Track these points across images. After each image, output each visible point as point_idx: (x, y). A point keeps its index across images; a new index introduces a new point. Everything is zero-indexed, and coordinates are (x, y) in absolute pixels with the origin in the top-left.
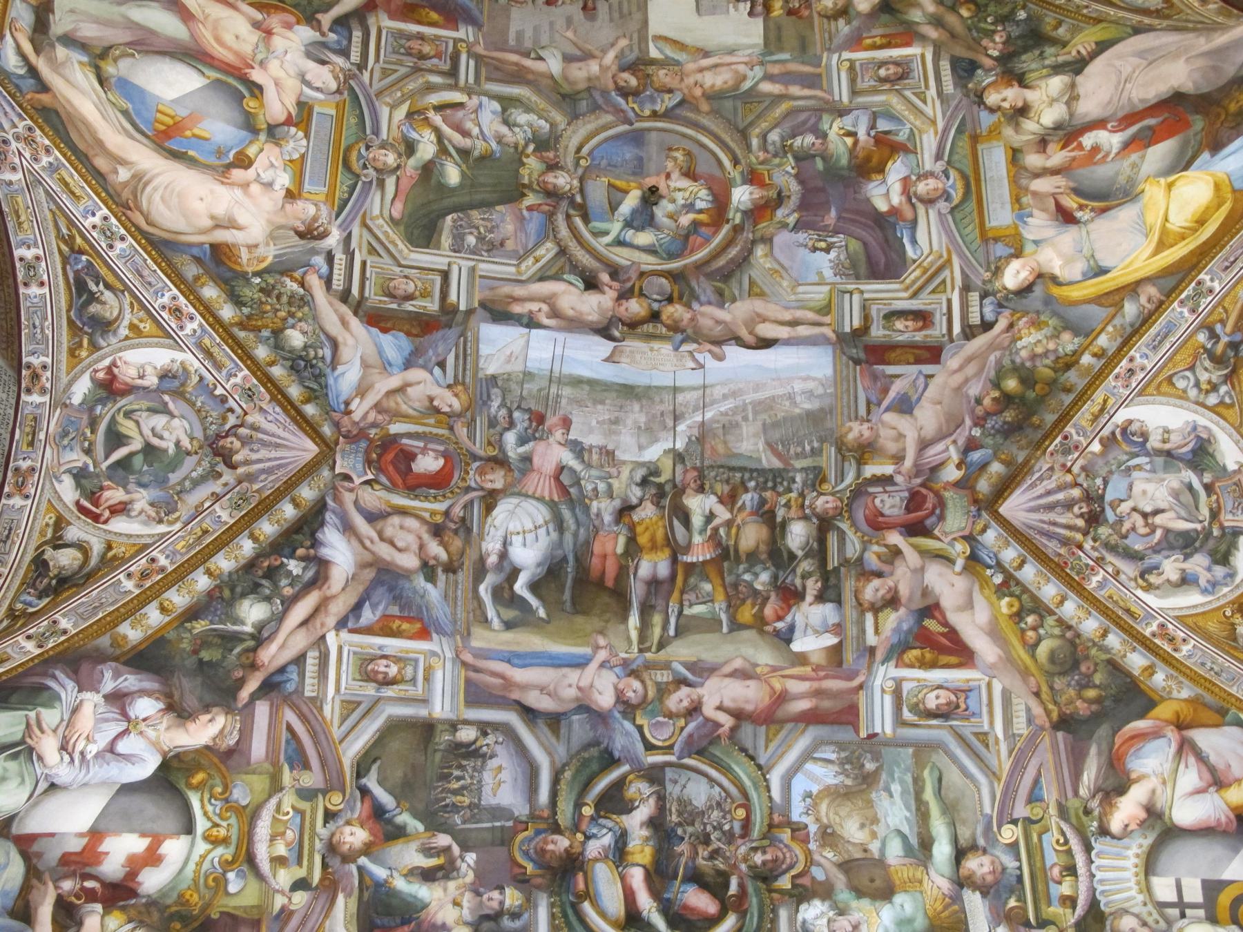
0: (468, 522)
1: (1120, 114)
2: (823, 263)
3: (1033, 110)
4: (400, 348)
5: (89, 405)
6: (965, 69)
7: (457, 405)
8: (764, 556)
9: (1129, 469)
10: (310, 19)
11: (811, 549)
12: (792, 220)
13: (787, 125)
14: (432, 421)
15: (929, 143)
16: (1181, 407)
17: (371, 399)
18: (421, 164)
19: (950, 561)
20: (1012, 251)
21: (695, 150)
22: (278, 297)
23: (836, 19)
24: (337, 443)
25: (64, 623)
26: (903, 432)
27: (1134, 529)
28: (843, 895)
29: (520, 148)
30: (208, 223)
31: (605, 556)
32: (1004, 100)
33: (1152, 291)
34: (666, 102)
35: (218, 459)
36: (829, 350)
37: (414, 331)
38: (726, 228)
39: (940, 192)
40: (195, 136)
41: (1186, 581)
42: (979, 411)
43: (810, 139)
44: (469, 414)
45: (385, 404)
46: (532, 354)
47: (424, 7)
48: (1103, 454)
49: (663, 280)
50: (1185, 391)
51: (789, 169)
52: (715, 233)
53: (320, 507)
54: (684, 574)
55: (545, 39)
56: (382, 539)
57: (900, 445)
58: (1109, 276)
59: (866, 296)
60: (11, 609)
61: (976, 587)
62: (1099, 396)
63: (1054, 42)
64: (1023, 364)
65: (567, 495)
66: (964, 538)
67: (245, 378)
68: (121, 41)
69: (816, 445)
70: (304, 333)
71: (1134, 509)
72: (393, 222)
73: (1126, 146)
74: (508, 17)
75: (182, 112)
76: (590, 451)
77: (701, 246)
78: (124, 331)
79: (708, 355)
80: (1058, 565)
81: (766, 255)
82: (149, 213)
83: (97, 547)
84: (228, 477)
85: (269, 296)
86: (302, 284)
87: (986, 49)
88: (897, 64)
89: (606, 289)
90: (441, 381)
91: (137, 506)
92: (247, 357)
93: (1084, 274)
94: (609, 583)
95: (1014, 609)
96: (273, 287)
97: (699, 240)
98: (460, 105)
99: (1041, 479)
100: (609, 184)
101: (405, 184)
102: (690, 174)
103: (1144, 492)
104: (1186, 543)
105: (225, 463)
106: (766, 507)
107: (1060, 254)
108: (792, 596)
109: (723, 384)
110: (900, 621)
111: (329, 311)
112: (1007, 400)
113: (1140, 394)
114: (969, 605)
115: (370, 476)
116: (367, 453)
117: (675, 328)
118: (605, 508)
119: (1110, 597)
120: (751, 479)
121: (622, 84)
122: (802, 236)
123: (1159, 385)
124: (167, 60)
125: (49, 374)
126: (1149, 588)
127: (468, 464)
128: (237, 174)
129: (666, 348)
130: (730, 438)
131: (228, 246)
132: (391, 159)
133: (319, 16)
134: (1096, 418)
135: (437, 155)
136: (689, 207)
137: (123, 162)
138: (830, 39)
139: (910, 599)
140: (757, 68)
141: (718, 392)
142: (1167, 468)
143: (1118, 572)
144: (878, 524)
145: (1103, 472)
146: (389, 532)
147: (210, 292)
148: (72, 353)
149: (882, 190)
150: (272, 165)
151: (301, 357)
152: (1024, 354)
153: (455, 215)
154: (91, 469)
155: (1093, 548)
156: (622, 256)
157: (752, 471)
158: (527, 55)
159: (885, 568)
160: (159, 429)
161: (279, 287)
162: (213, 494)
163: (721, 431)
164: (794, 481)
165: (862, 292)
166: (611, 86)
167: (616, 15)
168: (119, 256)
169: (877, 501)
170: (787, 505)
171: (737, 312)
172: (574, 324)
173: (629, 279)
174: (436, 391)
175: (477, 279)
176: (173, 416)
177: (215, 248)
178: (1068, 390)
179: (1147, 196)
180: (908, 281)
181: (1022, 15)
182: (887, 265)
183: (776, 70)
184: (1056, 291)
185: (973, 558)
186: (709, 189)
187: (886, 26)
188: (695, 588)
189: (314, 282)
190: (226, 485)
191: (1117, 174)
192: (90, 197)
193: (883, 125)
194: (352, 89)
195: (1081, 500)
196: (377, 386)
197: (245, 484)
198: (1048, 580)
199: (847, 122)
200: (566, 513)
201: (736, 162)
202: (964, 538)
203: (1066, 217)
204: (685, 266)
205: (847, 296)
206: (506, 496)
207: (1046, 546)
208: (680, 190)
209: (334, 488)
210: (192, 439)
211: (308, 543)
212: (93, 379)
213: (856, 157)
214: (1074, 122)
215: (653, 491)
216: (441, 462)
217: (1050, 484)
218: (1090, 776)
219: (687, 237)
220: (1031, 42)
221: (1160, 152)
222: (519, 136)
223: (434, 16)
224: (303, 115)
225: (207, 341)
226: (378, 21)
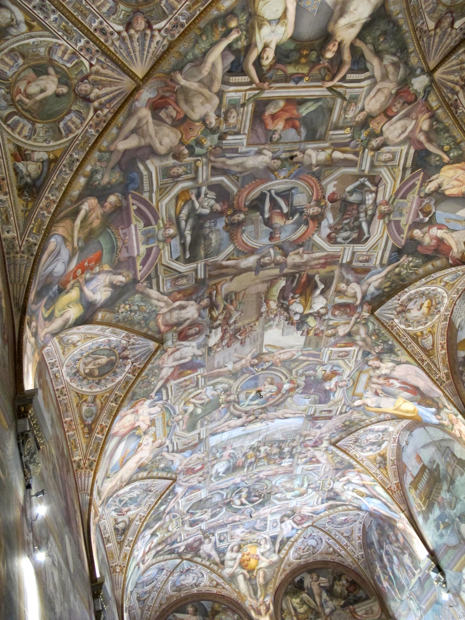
6: (366, 354)
10: (148, 397)
15: (347, 372)
25: (131, 539)
28: (284, 492)
38: (280, 395)
41: (371, 450)
43: (311, 372)
54: (258, 459)
60: (118, 542)
73: (400, 388)
83: (127, 520)
84: (151, 493)
101: (185, 420)
102: (271, 384)
104: (374, 444)
108: (282, 458)
114: (323, 456)
117: (262, 419)
122: (302, 395)
126: (362, 451)
136: (270, 392)
147: (141, 475)
156: (248, 408)
158: (221, 368)
167: (252, 342)
171: (280, 412)
183: (305, 353)
184: (366, 408)
193: (335, 368)
199: (324, 368)
201: (287, 378)
203: (377, 394)
218: (338, 475)
223: (189, 372)
224: (153, 422)
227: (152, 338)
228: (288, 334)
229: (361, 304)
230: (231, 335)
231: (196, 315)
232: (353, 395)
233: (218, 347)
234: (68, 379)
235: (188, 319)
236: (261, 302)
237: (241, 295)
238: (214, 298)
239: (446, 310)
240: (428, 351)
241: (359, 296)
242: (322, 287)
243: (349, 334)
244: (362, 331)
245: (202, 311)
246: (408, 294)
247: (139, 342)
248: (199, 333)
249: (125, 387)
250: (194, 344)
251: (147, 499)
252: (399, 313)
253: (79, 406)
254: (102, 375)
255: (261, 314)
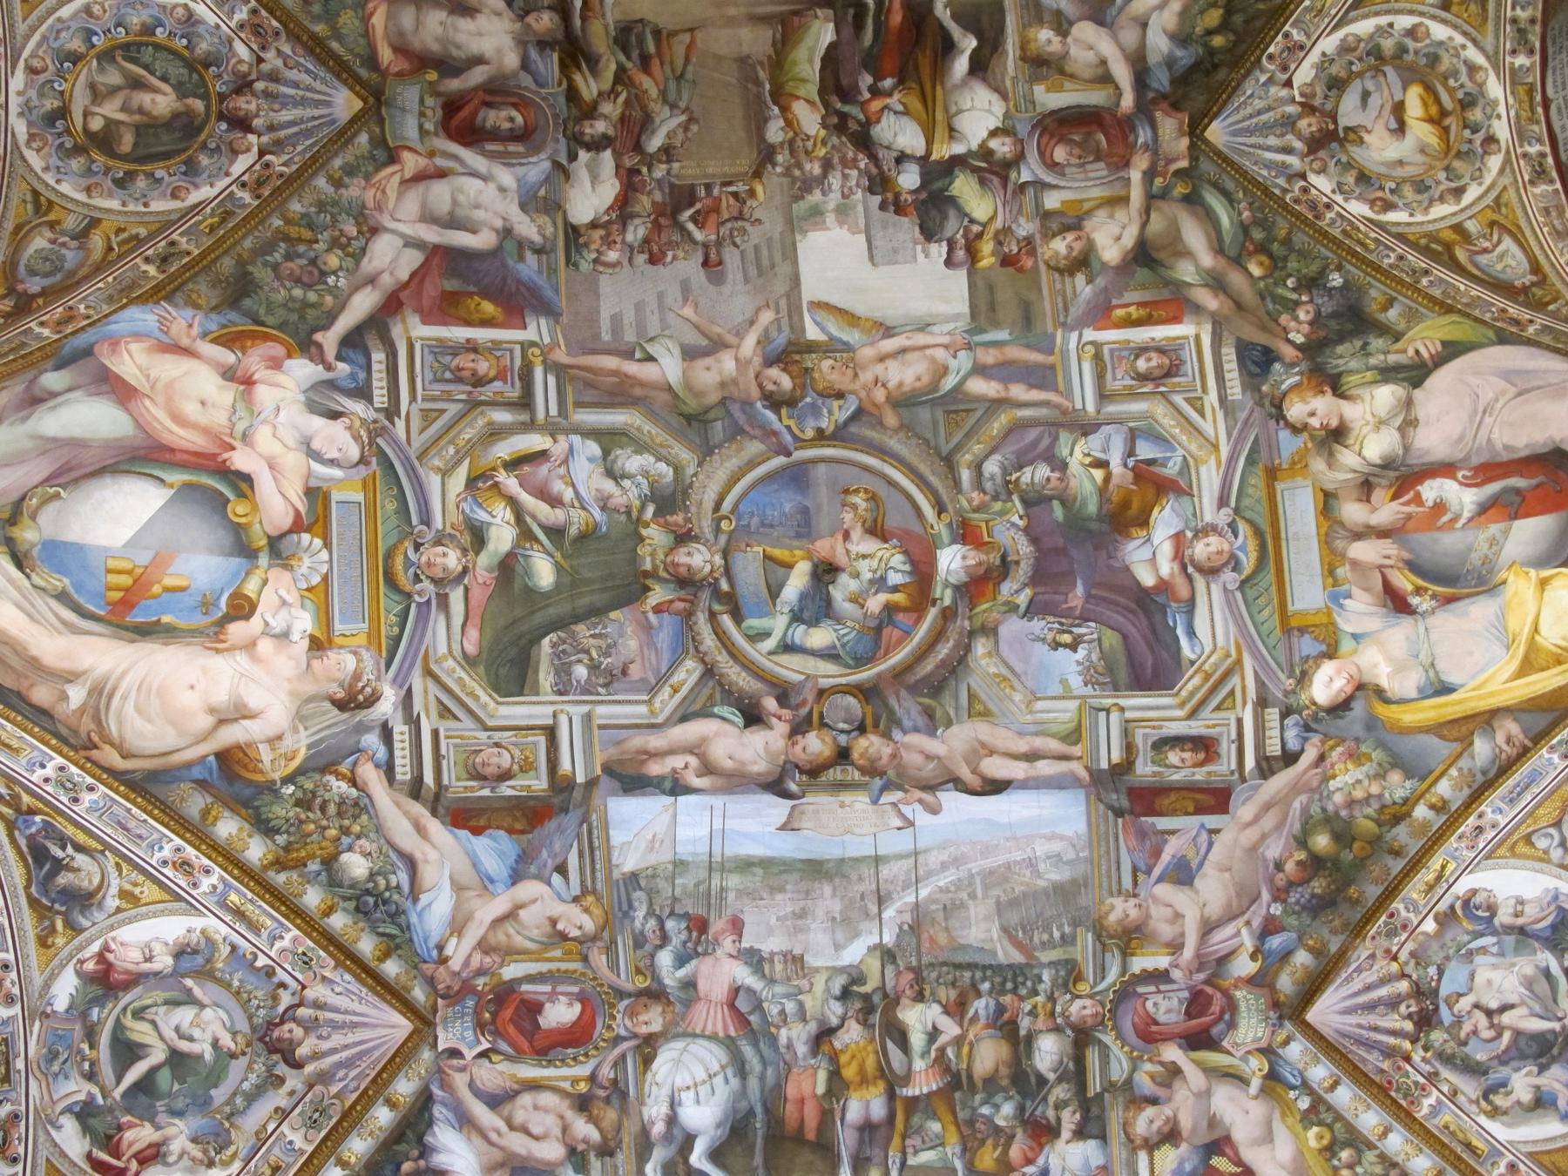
0: (621, 1085)
1: (1475, 461)
2: (1069, 666)
3: (1354, 434)
4: (502, 855)
5: (79, 1009)
6: (1257, 362)
7: (589, 925)
8: (1005, 1082)
9: (1470, 953)
10: (306, 346)
11: (1066, 1071)
12: (1023, 599)
13: (1009, 449)
14: (558, 953)
15: (1209, 479)
16: (1541, 871)
17: (473, 935)
18: (496, 561)
19: (1243, 1081)
20: (1324, 648)
21: (882, 490)
22: (323, 808)
23: (1072, 274)
24: (435, 1011)
26: (1180, 910)
27: (1475, 1032)
29: (635, 514)
30: (206, 721)
31: (802, 1101)
32: (1312, 414)
33: (1511, 727)
34: (836, 414)
35: (276, 1057)
36: (1081, 795)
37: (518, 826)
38: (932, 613)
39: (1226, 556)
40: (167, 590)
42: (1280, 879)
43: (1043, 471)
44: (606, 935)
45: (492, 940)
46: (683, 833)
47: (471, 294)
48: (1439, 934)
49: (851, 699)
50: (1546, 852)
51: (1015, 519)
52: (918, 621)
53: (425, 1100)
55: (653, 328)
56: (512, 1127)
57: (1176, 929)
58: (1454, 696)
59: (1128, 715)
61: (1277, 1115)
62: (1436, 863)
63: (1384, 330)
64: (1337, 813)
65: (747, 1024)
66: (1260, 1050)
67: (295, 940)
68: (38, 478)
69: (1067, 930)
70: (367, 855)
71: (1477, 1006)
72: (469, 661)
73: (1484, 509)
74: (597, 295)
75: (143, 558)
76: (772, 961)
77: (899, 642)
78: (112, 903)
79: (917, 806)
80: (1380, 1087)
81: (989, 654)
82: (122, 740)
84: (294, 1081)
85: (309, 809)
86: (353, 782)
87: (1286, 330)
88: (1161, 351)
89: (774, 721)
90: (565, 895)
91: (175, 1147)
92: (296, 913)
93: (1420, 690)
94: (811, 1135)
95: (1325, 1142)
96: (314, 793)
97: (896, 633)
98: (542, 455)
99: (1359, 970)
100: (767, 557)
101: (478, 595)
102: (876, 530)
103: (1489, 983)
105: (286, 1062)
106: (1006, 1016)
107: (1389, 659)
108: (1044, 1133)
109: (942, 847)
110: (1181, 1162)
111: (397, 816)
112: (1316, 864)
113: (1488, 857)
114: (1268, 1137)
115: (485, 1045)
116: (477, 1012)
117: (872, 770)
118: (796, 1036)
119: (1446, 1127)
120: (984, 979)
121: (770, 387)
122: (1038, 625)
123: (1515, 845)
124: (108, 480)
125: (14, 975)
127: (612, 1006)
128: (236, 630)
129: (859, 802)
130: (953, 923)
131: (239, 747)
132: (452, 559)
133: (318, 337)
134: (1431, 888)
135: (517, 544)
136: (880, 583)
137: (71, 677)
138: (1066, 309)
139: (1194, 1130)
140: (962, 354)
141: (934, 859)
142: (1518, 949)
143: (1455, 1093)
144: (1150, 1034)
145: (1438, 959)
146: (520, 1117)
147: (227, 827)
148: (43, 942)
149: (1145, 553)
150: (284, 603)
151: (368, 892)
152: (1338, 798)
153: (553, 637)
154: (100, 1101)
155: (1424, 1059)
156: (791, 668)
157: (984, 968)
158: (628, 354)
159: (1161, 1092)
160: (185, 1026)
161: (321, 792)
162: (277, 1110)
163: (940, 916)
164: (1040, 980)
165: (1122, 709)
166: (755, 392)
167: (753, 271)
168: (88, 810)
169: (1149, 1005)
170: (1033, 1013)
171: (954, 742)
172: (735, 781)
173: (804, 702)
174: (558, 909)
175: (596, 732)
176: (203, 1006)
177: (223, 756)
178: (1397, 853)
179: (1510, 589)
180: (1184, 693)
181: (1336, 280)
182: (1155, 668)
183: (989, 357)
184: (1381, 710)
185: (1273, 1076)
186: (906, 553)
187: (1143, 287)
188: (920, 1130)
189: (370, 775)
190: (292, 1093)
191: (1470, 549)
192: (34, 748)
193: (1145, 451)
194: (382, 454)
195: (1409, 996)
196: (478, 915)
197: (318, 1088)
198: (1369, 1107)
199: (1094, 443)
200: (748, 1051)
201: (940, 509)
202: (1261, 1051)
203: (1397, 603)
204: (879, 675)
205: (1102, 715)
206: (667, 1040)
207: (1364, 1060)
208: (864, 557)
209: (440, 1071)
210: (234, 1034)
211: (416, 1153)
212: (78, 973)
213: (1109, 500)
214: (1410, 461)
215: (858, 1005)
216: (578, 1008)
217: (1370, 977)
219: (878, 630)
220: (1350, 326)
221: (1531, 531)
222: (628, 495)
223: (488, 308)
224: (316, 512)
225: (233, 897)
226: (406, 330)
227: (341, 70)
228: (893, 257)
229: (1145, 108)
230: (658, 210)
231: (512, 60)
232: (1287, 630)
233: (609, 243)
234: (21, 128)
235: (479, 60)
236: (759, 96)
237: (679, 51)
238: (578, 22)
239: (1521, 135)
240: (1525, 290)
241: (1122, 73)
242: (969, 43)
243: (1144, 256)
244: (1194, 237)
245: (534, 54)
246: (1314, 57)
247: (293, 75)
248: (522, 136)
249: (212, 229)
250: (506, 177)
251: (261, 1111)
252: (1315, 144)
253: (20, 234)
254: (142, 157)
255: (767, 155)
